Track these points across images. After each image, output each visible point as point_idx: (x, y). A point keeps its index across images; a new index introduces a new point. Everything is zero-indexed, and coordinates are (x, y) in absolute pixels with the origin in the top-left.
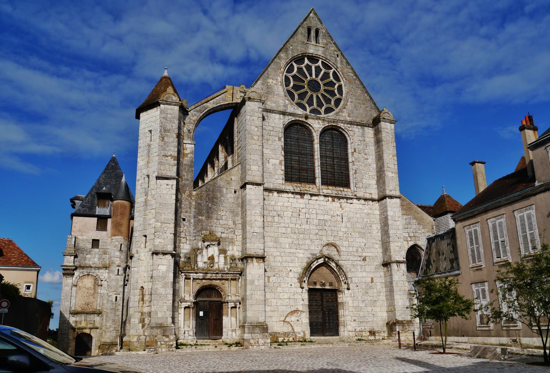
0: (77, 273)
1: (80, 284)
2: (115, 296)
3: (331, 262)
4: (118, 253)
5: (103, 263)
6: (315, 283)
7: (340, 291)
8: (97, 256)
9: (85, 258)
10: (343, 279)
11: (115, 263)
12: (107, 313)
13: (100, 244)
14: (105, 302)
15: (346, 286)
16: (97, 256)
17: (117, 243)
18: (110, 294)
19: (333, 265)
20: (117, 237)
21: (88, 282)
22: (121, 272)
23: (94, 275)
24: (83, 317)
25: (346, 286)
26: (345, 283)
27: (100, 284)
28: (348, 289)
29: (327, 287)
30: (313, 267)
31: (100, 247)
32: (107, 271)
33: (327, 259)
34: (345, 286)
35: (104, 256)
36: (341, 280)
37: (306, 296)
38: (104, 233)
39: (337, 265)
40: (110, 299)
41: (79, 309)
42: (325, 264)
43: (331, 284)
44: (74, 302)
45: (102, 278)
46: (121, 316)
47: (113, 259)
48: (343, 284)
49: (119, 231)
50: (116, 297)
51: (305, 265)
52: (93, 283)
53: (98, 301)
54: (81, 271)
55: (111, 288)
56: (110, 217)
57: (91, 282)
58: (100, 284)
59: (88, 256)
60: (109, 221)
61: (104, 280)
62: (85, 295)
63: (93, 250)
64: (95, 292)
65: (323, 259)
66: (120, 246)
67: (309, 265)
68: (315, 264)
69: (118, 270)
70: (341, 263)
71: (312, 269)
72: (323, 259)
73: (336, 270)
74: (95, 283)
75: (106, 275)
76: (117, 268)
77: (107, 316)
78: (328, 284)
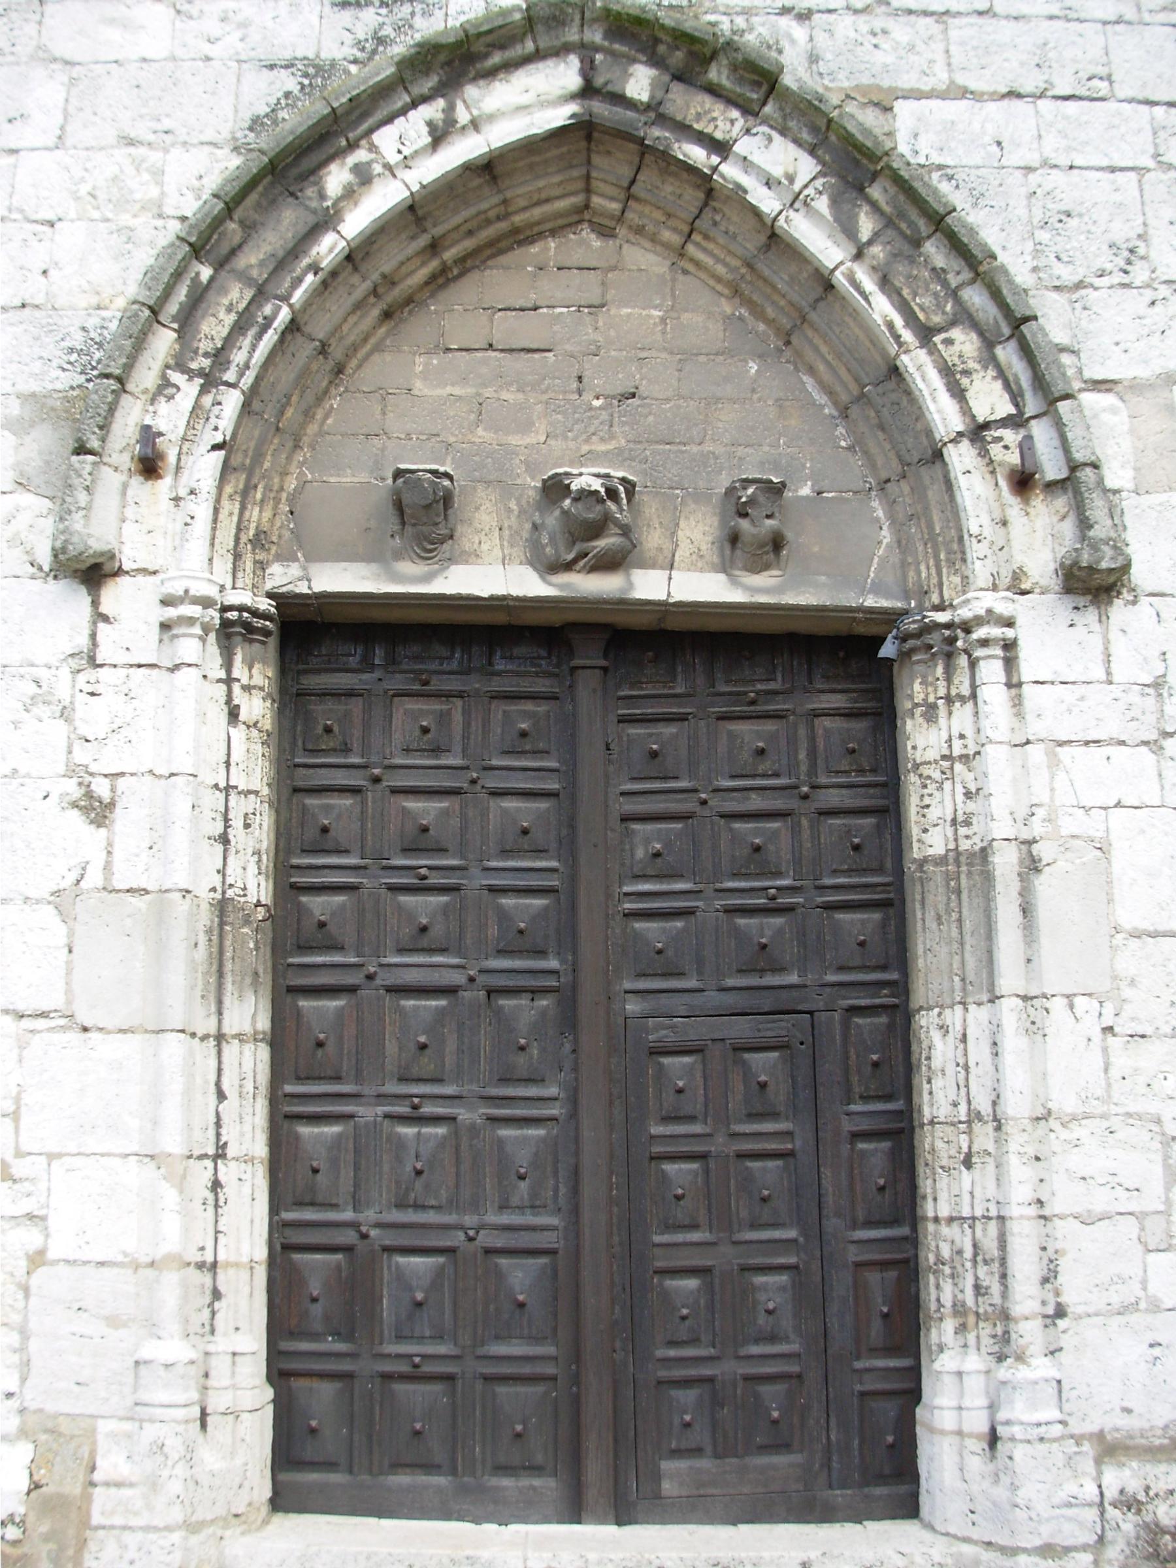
3: (725, 122)
6: (423, 514)
7: (948, 643)
10: (989, 399)
15: (1038, 538)
19: (767, 166)
25: (1038, 538)
26: (1023, 482)
28: (1093, 584)
29: (684, 576)
30: (357, 222)
33: (639, 83)
34: (1008, 542)
36: (944, 415)
37: (195, 745)
39: (855, 164)
42: (603, 168)
43: (753, 526)
48: (975, 486)
51: (196, 175)
65: (565, 75)
67: (287, 168)
68: (406, 159)
70: (918, 136)
71: (328, 248)
72: (565, 75)
73: (816, 237)
78: (699, 530)
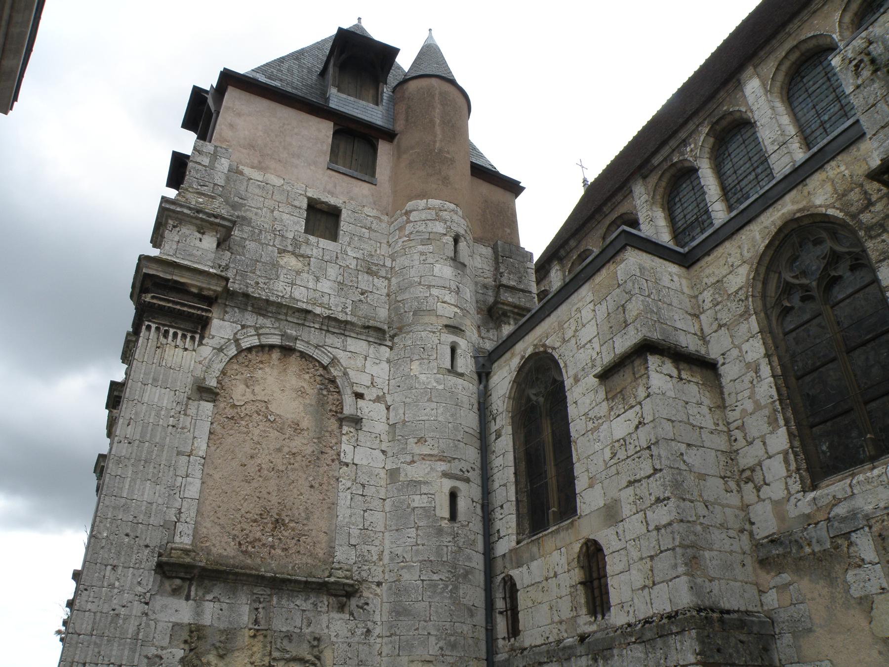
0: (222, 328)
1: (239, 392)
2: (447, 485)
4: (445, 271)
5: (364, 309)
8: (333, 271)
9: (275, 266)
11: (432, 312)
12: (398, 590)
13: (344, 226)
14: (377, 519)
16: (333, 271)
17: (439, 228)
18: (417, 472)
20: (435, 202)
21: (282, 391)
22: (466, 364)
23: (316, 354)
24: (242, 610)
27: (348, 410)
31: (343, 238)
32: (385, 352)
35: (364, 281)
38: (362, 189)
40: (418, 501)
41: (223, 548)
44: (193, 489)
45: (361, 380)
46: (480, 617)
47: (420, 292)
49: (445, 181)
50: (453, 496)
52: (311, 399)
53: (343, 511)
54: (250, 319)
55: (421, 440)
56: (389, 136)
57: (302, 392)
58: (348, 410)
59: (291, 261)
60: (384, 149)
61: (370, 394)
62: (263, 459)
63: (312, 239)
64: (325, 456)
66: (449, 240)
69: (453, 350)
74: (321, 402)
75: (381, 371)
76: (452, 338)
77: (399, 612)
